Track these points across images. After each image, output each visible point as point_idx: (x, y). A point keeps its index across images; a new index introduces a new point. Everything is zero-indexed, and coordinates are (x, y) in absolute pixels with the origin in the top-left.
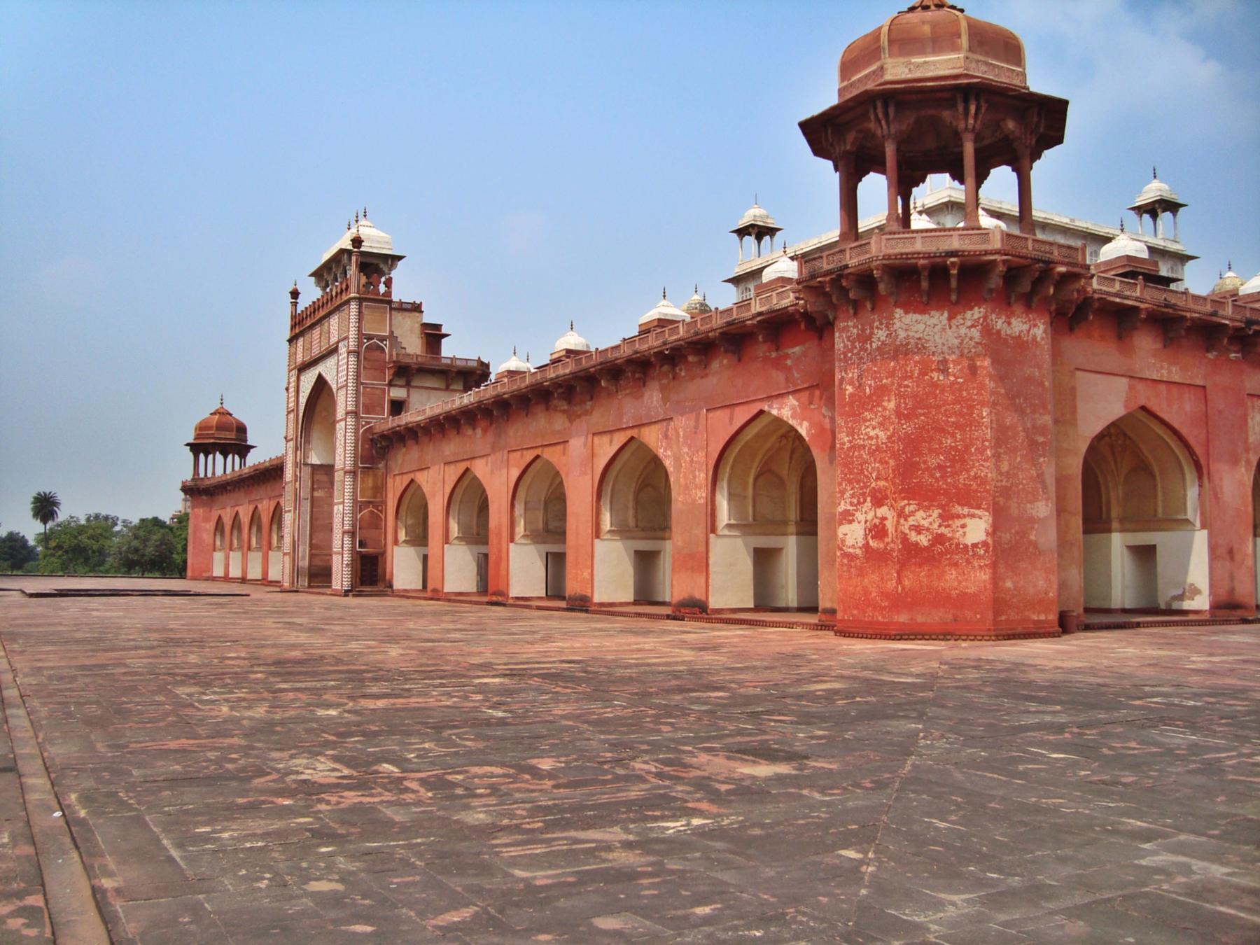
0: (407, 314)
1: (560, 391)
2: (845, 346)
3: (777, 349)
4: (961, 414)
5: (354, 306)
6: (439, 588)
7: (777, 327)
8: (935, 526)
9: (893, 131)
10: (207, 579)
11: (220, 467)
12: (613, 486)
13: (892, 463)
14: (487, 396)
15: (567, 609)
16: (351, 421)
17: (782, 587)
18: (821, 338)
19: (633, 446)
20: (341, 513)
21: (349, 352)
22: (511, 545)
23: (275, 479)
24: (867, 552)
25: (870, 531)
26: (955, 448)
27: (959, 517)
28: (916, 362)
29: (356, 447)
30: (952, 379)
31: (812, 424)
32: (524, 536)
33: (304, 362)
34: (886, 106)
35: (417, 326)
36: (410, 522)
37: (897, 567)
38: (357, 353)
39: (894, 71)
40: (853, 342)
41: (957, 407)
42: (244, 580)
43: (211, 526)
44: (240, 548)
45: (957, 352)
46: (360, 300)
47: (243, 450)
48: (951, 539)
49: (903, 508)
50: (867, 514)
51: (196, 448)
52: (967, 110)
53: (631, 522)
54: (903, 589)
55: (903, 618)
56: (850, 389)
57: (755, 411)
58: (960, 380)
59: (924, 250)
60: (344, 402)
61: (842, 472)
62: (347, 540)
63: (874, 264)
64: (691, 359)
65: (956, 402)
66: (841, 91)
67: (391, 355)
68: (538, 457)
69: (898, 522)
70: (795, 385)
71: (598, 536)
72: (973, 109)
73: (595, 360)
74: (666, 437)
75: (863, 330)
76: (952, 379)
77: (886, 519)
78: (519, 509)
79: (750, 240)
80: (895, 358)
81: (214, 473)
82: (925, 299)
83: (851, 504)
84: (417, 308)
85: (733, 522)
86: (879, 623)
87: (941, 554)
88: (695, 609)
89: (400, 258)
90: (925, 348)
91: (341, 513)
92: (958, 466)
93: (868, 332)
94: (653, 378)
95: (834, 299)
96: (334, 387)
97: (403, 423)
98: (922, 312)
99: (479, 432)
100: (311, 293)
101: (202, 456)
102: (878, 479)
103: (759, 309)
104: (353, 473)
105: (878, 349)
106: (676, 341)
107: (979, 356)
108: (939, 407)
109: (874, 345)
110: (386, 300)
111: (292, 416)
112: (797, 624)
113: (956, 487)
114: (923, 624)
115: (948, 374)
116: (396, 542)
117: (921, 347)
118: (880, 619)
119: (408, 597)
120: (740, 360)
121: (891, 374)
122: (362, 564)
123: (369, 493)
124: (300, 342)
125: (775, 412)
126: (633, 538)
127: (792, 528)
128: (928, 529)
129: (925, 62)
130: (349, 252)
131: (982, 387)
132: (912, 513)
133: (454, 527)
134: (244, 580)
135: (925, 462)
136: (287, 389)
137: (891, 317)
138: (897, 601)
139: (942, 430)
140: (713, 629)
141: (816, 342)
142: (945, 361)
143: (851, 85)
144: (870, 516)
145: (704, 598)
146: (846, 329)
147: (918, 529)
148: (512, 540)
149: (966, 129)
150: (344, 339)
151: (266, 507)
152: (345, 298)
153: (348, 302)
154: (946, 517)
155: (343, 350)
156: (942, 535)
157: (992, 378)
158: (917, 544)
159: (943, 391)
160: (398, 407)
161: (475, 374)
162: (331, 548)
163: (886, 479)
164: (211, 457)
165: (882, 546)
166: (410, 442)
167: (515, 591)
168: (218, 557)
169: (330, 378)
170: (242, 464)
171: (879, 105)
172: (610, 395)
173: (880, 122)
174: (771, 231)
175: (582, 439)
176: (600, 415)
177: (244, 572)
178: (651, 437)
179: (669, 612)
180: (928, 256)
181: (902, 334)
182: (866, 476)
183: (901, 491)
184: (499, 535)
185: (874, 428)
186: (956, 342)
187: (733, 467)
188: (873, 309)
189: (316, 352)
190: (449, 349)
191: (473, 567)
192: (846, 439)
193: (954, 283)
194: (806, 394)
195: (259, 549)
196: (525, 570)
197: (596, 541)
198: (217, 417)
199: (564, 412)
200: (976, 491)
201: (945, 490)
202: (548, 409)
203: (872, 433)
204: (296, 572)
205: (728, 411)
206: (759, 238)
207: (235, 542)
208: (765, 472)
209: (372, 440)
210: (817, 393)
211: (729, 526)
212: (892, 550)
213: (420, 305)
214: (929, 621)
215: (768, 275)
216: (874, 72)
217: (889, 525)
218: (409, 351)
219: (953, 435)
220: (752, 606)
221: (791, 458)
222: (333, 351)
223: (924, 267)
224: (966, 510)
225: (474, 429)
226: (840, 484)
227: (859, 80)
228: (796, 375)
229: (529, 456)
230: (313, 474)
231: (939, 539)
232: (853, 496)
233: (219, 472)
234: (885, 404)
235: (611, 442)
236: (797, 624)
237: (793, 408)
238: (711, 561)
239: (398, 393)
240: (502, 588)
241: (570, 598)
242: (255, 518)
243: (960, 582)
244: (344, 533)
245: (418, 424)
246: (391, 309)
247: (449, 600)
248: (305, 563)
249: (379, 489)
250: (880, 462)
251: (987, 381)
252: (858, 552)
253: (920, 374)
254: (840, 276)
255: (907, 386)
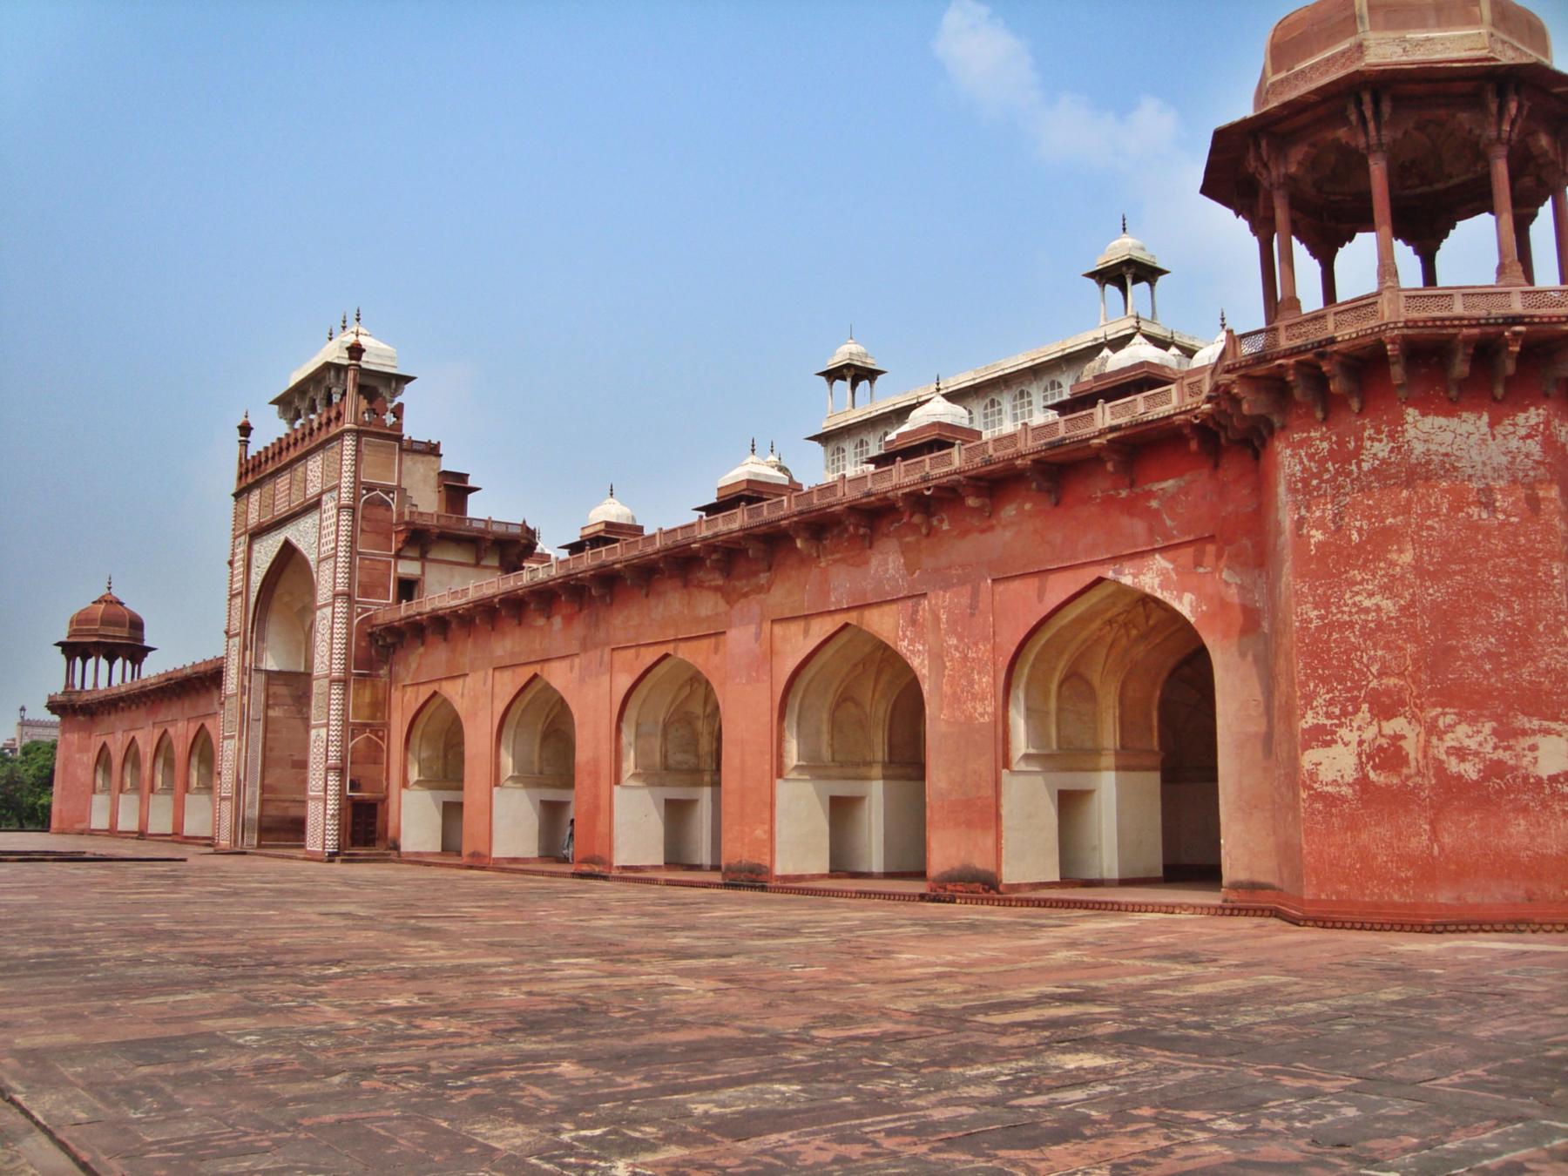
0: (418, 457)
1: (714, 557)
2: (1304, 470)
3: (1132, 485)
4: (1517, 572)
5: (349, 442)
6: (483, 849)
7: (1143, 449)
8: (1488, 748)
9: (1387, 136)
10: (81, 833)
11: (103, 676)
12: (803, 698)
13: (1411, 648)
14: (582, 567)
15: (726, 886)
16: (341, 606)
17: (1094, 848)
18: (1216, 466)
19: (844, 637)
20: (324, 740)
21: (340, 508)
22: (617, 789)
23: (198, 692)
24: (1364, 790)
25: (1370, 757)
26: (1513, 625)
27: (1524, 733)
28: (1444, 491)
29: (348, 644)
30: (1501, 517)
31: (1201, 596)
32: (634, 775)
33: (260, 524)
34: (1376, 103)
35: (433, 480)
36: (424, 755)
37: (1430, 813)
38: (352, 509)
39: (1380, 51)
40: (1322, 463)
41: (1512, 561)
42: (142, 835)
43: (90, 757)
44: (137, 788)
45: (1506, 476)
46: (359, 434)
47: (136, 652)
48: (1514, 769)
49: (1437, 716)
50: (1361, 730)
51: (73, 650)
52: (1502, 109)
53: (826, 753)
54: (1442, 849)
55: (1445, 896)
56: (1317, 535)
57: (1089, 580)
58: (1513, 519)
59: (1467, 314)
60: (328, 580)
61: (1306, 665)
62: (333, 779)
63: (1388, 334)
64: (971, 502)
65: (1511, 552)
66: (1261, 94)
67: (401, 514)
68: (666, 656)
69: (1428, 742)
70: (1166, 537)
71: (780, 775)
72: (1513, 107)
73: (788, 505)
74: (913, 622)
75: (1341, 443)
76: (1501, 517)
77: (1403, 737)
78: (628, 735)
79: (843, 386)
80: (1408, 484)
81: (96, 684)
82: (1453, 393)
83: (1328, 715)
84: (432, 450)
85: (1032, 751)
86: (1394, 905)
87: (1500, 792)
88: (982, 885)
89: (408, 379)
90: (1456, 469)
91: (324, 740)
92: (1518, 654)
93: (1352, 445)
94: (887, 535)
95: (1334, 387)
96: (312, 558)
97: (428, 608)
98: (1449, 414)
99: (557, 621)
100: (271, 429)
101: (78, 661)
102: (1381, 675)
103: (1110, 421)
104: (344, 682)
105: (1374, 471)
106: (947, 474)
107: (1541, 482)
108: (1486, 561)
109: (1365, 466)
110: (394, 435)
111: (238, 601)
112: (1182, 907)
113: (1517, 687)
114: (1476, 906)
115: (1495, 510)
116: (405, 783)
117: (1449, 467)
118: (1396, 897)
119: (428, 864)
120: (1057, 504)
121: (1406, 509)
122: (355, 815)
123: (366, 712)
124: (255, 496)
125: (1127, 580)
126: (828, 778)
127: (1109, 760)
128: (1477, 754)
129: (1428, 39)
130: (340, 369)
131: (1550, 529)
132: (1450, 728)
133: (507, 762)
134: (142, 835)
135: (1466, 647)
136: (231, 563)
137: (1400, 420)
138: (1428, 870)
139: (1490, 597)
140: (744, 903)
141: (1206, 472)
142: (1488, 490)
143: (1296, 75)
144: (1370, 733)
145: (991, 868)
146: (1306, 442)
147: (1460, 753)
148: (618, 781)
149: (1499, 139)
150: (330, 490)
151: (182, 732)
152: (334, 430)
153: (340, 436)
154: (1505, 734)
155: (329, 504)
156: (1500, 762)
157: (1560, 512)
158: (1460, 777)
159: (1488, 536)
160: (407, 588)
161: (514, 547)
162: (305, 790)
163: (1401, 675)
164: (91, 662)
165: (1395, 781)
166: (430, 638)
167: (621, 858)
168: (100, 802)
169: (301, 546)
170: (136, 673)
171: (1367, 98)
172: (804, 561)
173: (1363, 121)
174: (871, 374)
175: (752, 629)
176: (784, 593)
177: (143, 822)
178: (884, 624)
179: (923, 891)
180: (1476, 322)
181: (1419, 448)
182: (1359, 672)
183: (1431, 693)
184: (595, 774)
185: (1371, 595)
186: (1504, 460)
187: (1033, 666)
188: (1361, 410)
189: (282, 508)
190: (478, 508)
191: (438, 820)
192: (1313, 614)
193: (1510, 367)
194: (1187, 554)
195: (165, 791)
196: (634, 825)
197: (779, 782)
198: (103, 606)
199: (717, 589)
200: (1549, 693)
201: (1502, 692)
202: (685, 586)
203: (1367, 603)
204: (240, 825)
205: (1034, 583)
206: (854, 386)
207: (128, 780)
208: (1074, 677)
209: (371, 635)
210: (1211, 549)
211: (1027, 757)
212: (1419, 787)
213: (437, 446)
214: (1486, 900)
215: (917, 419)
216: (1343, 53)
217: (1410, 747)
218: (421, 509)
219: (1508, 605)
220: (1057, 878)
221: (1108, 656)
222: (315, 505)
223: (1468, 341)
224: (1536, 723)
225: (549, 618)
226: (1304, 685)
227: (1302, 71)
228: (1169, 523)
229: (650, 656)
230: (268, 684)
231: (1495, 769)
232: (1331, 702)
233: (103, 684)
234: (1393, 556)
235: (806, 632)
236: (1182, 907)
237: (1163, 573)
238: (1004, 812)
239: (409, 568)
240: (598, 851)
241: (729, 867)
242: (163, 747)
243: (1532, 838)
244: (328, 769)
245: (454, 612)
246: (402, 450)
247: (503, 870)
248: (253, 812)
249: (380, 706)
250: (1387, 647)
251: (1557, 521)
252: (1347, 791)
253: (1450, 508)
254: (1322, 356)
255: (1431, 528)
